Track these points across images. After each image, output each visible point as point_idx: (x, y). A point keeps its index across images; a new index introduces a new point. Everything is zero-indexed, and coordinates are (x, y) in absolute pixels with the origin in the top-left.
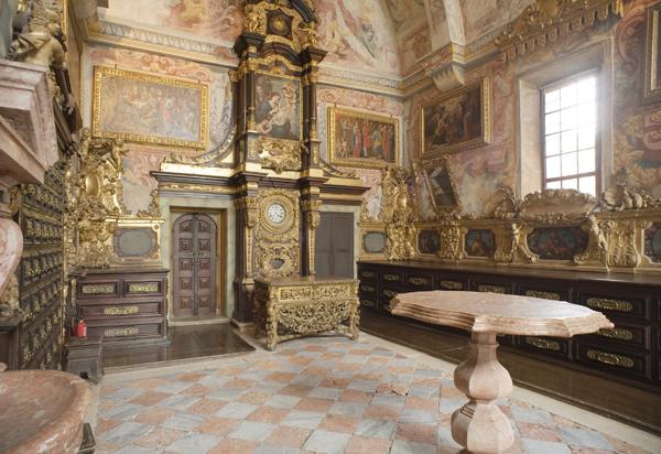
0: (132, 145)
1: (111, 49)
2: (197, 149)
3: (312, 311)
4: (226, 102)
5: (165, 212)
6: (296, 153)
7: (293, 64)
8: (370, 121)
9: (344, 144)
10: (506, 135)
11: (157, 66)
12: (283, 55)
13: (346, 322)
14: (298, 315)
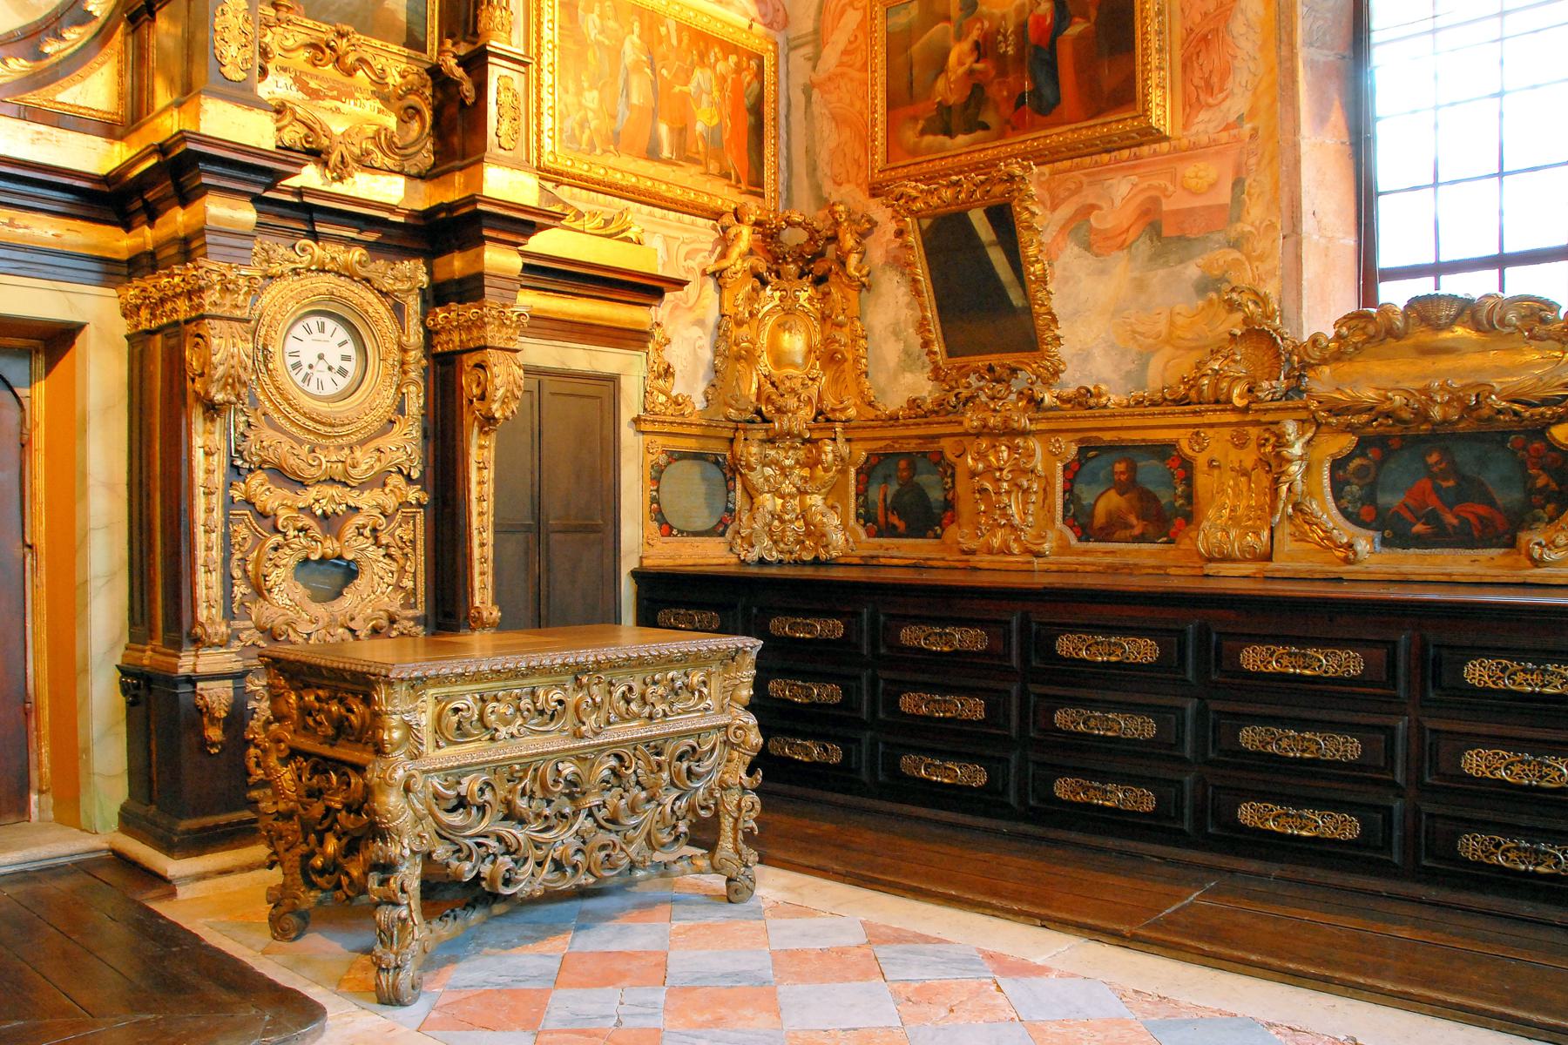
3: (574, 790)
6: (413, 100)
8: (681, 27)
9: (591, 98)
10: (1237, 104)
13: (704, 834)
14: (511, 815)
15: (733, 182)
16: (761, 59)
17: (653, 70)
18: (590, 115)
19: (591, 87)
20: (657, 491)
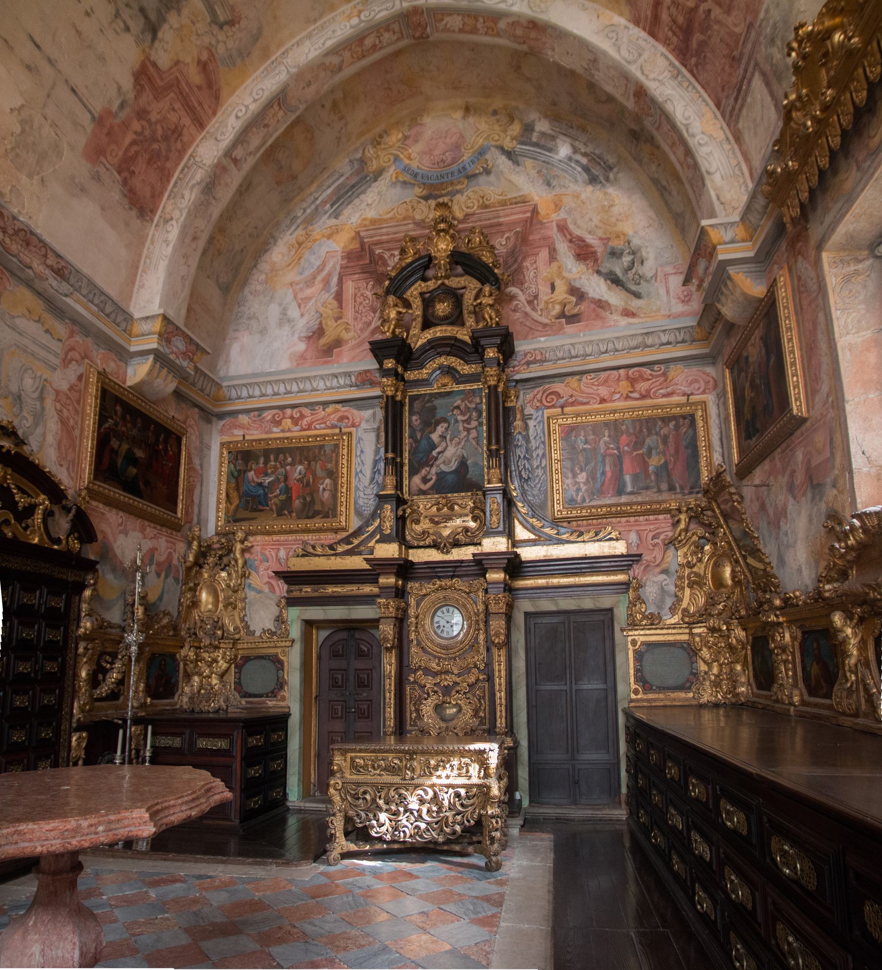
0: (259, 538)
1: (240, 416)
2: (336, 531)
4: (377, 451)
5: (295, 631)
7: (467, 362)
9: (582, 477)
11: (289, 421)
12: (448, 354)
15: (678, 490)
16: (692, 417)
17: (618, 448)
18: (582, 485)
19: (582, 470)
20: (641, 666)
